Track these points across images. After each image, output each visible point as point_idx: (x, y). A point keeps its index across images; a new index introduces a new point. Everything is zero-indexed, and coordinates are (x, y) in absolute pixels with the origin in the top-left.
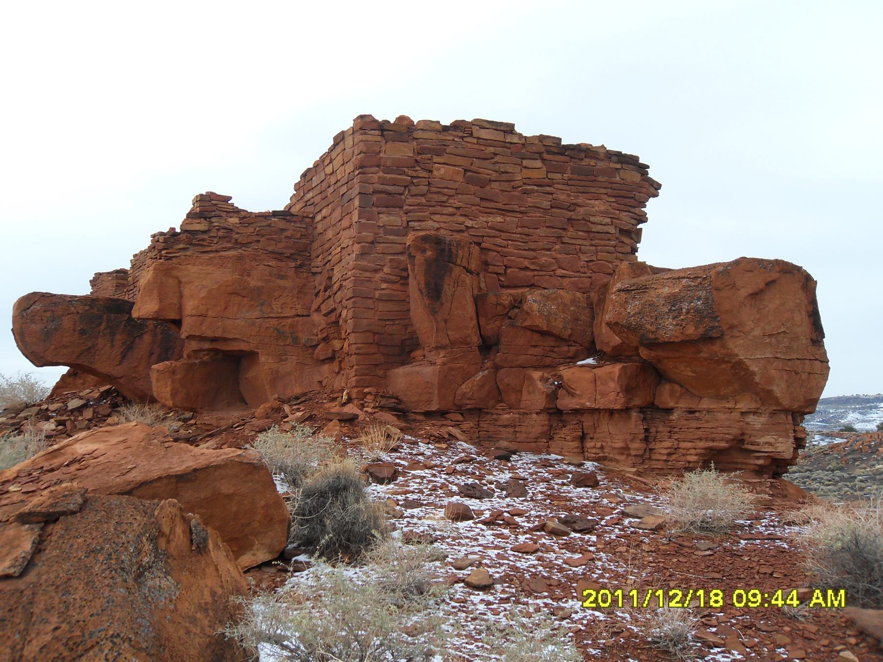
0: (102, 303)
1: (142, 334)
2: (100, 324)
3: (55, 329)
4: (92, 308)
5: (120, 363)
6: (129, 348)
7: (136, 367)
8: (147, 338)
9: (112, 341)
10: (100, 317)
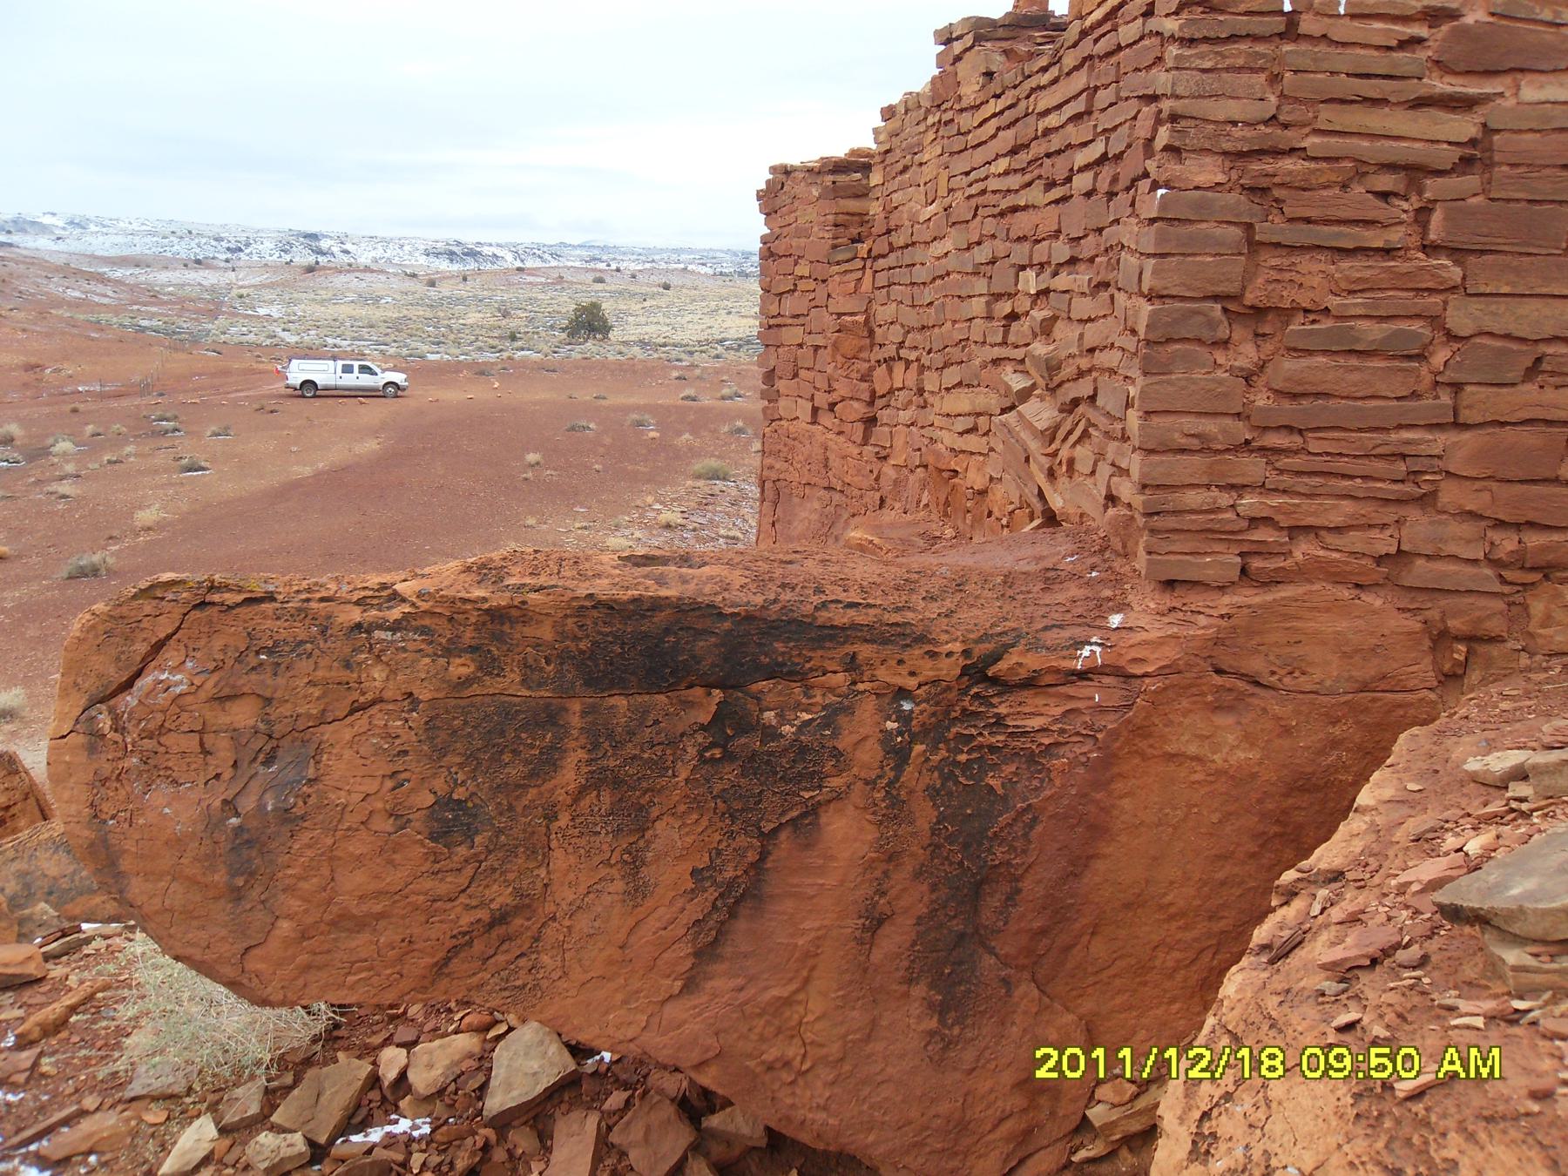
0: (546, 633)
1: (813, 810)
2: (548, 762)
3: (285, 815)
4: (490, 666)
5: (690, 985)
6: (734, 899)
7: (788, 1002)
8: (847, 832)
9: (634, 864)
10: (550, 717)
